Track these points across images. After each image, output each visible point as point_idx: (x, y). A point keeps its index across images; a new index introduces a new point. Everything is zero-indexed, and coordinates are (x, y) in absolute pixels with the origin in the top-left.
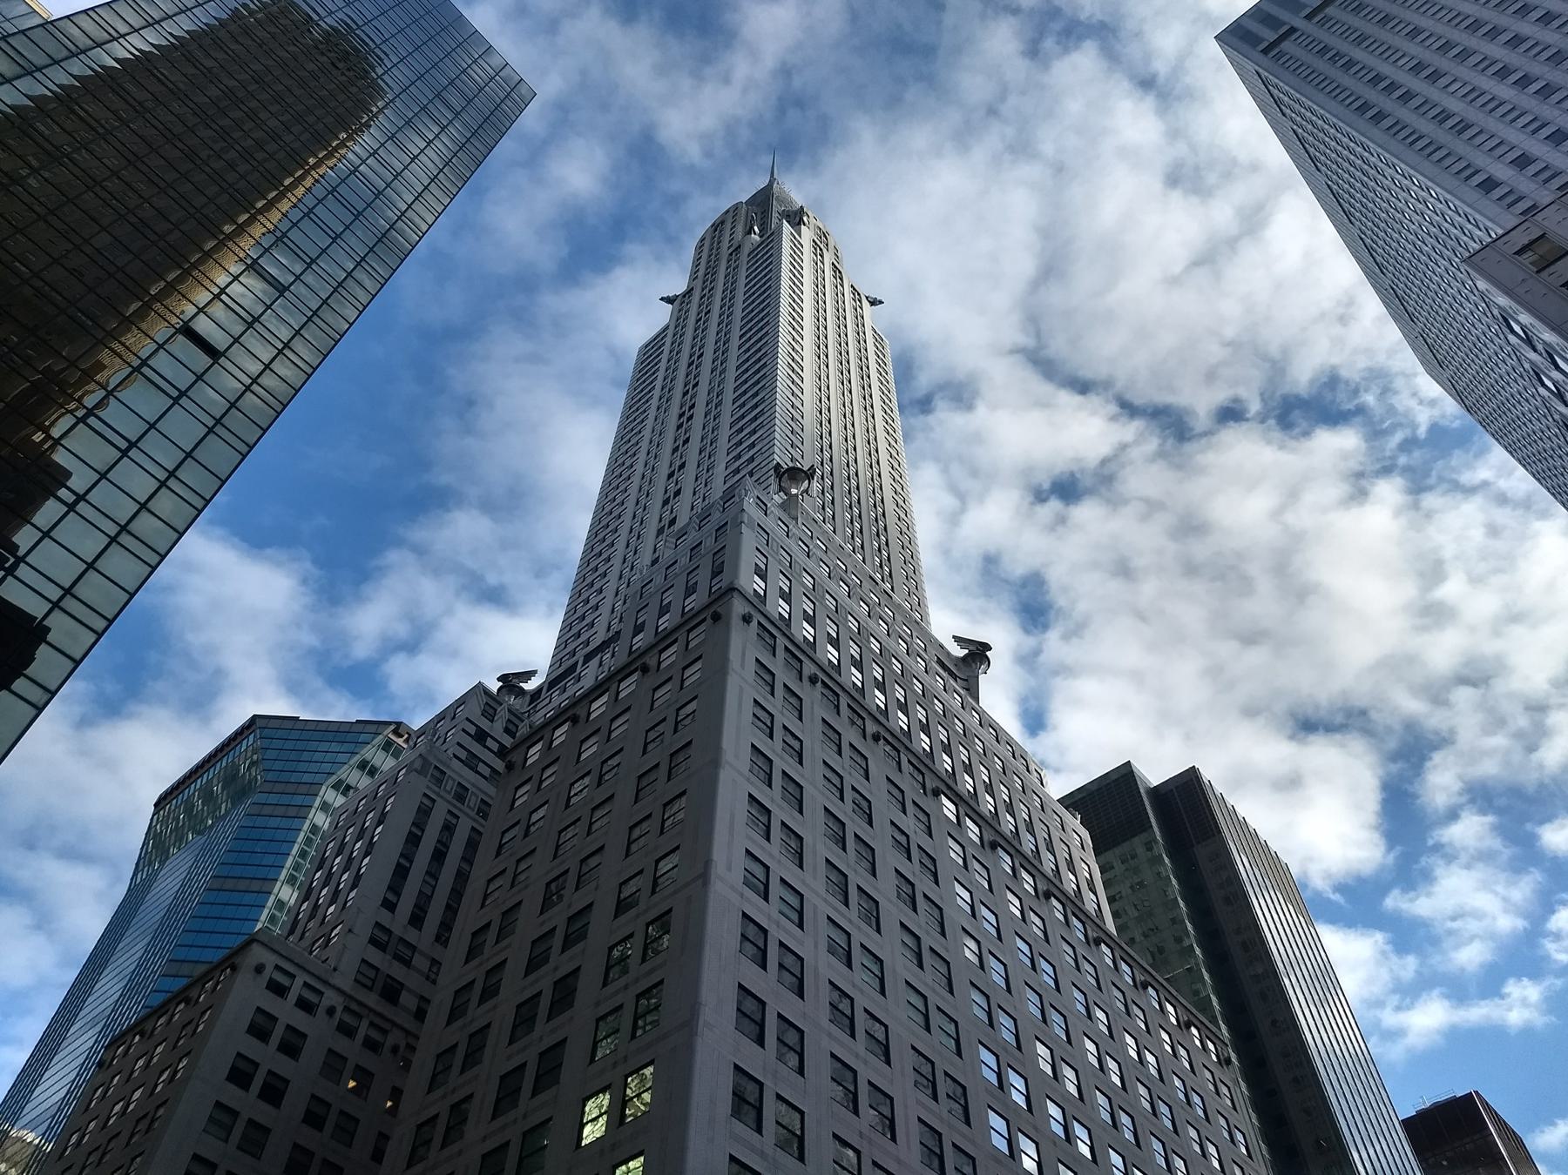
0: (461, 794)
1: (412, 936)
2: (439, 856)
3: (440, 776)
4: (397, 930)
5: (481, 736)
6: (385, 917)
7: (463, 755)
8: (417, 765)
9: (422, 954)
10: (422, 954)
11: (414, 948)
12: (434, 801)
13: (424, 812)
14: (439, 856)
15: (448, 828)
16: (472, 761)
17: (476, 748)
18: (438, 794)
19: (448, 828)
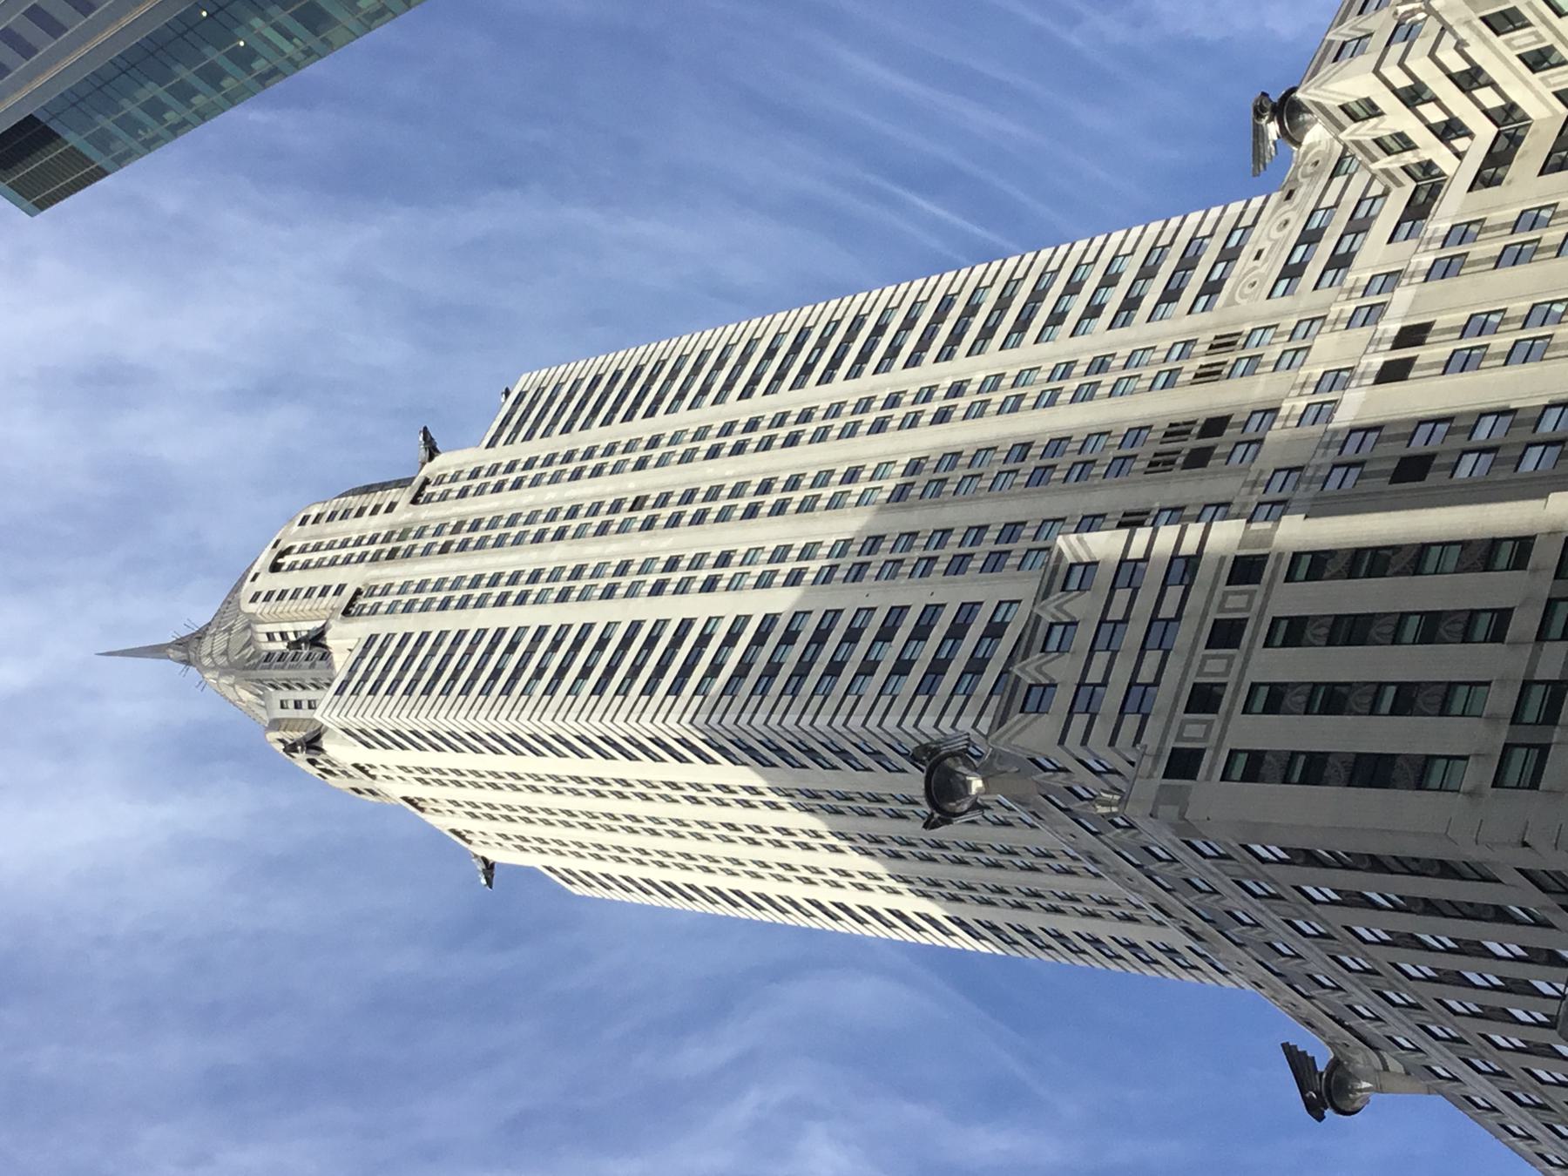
0: (1204, 699)
1: (1502, 700)
2: (1331, 699)
3: (1183, 764)
4: (1503, 735)
5: (1086, 696)
6: (1478, 774)
7: (1131, 722)
8: (1171, 811)
9: (1535, 657)
10: (1535, 657)
11: (1527, 685)
12: (1232, 752)
13: (1254, 766)
14: (1331, 699)
15: (1275, 699)
16: (1138, 696)
17: (1112, 699)
18: (1217, 750)
19: (1275, 699)
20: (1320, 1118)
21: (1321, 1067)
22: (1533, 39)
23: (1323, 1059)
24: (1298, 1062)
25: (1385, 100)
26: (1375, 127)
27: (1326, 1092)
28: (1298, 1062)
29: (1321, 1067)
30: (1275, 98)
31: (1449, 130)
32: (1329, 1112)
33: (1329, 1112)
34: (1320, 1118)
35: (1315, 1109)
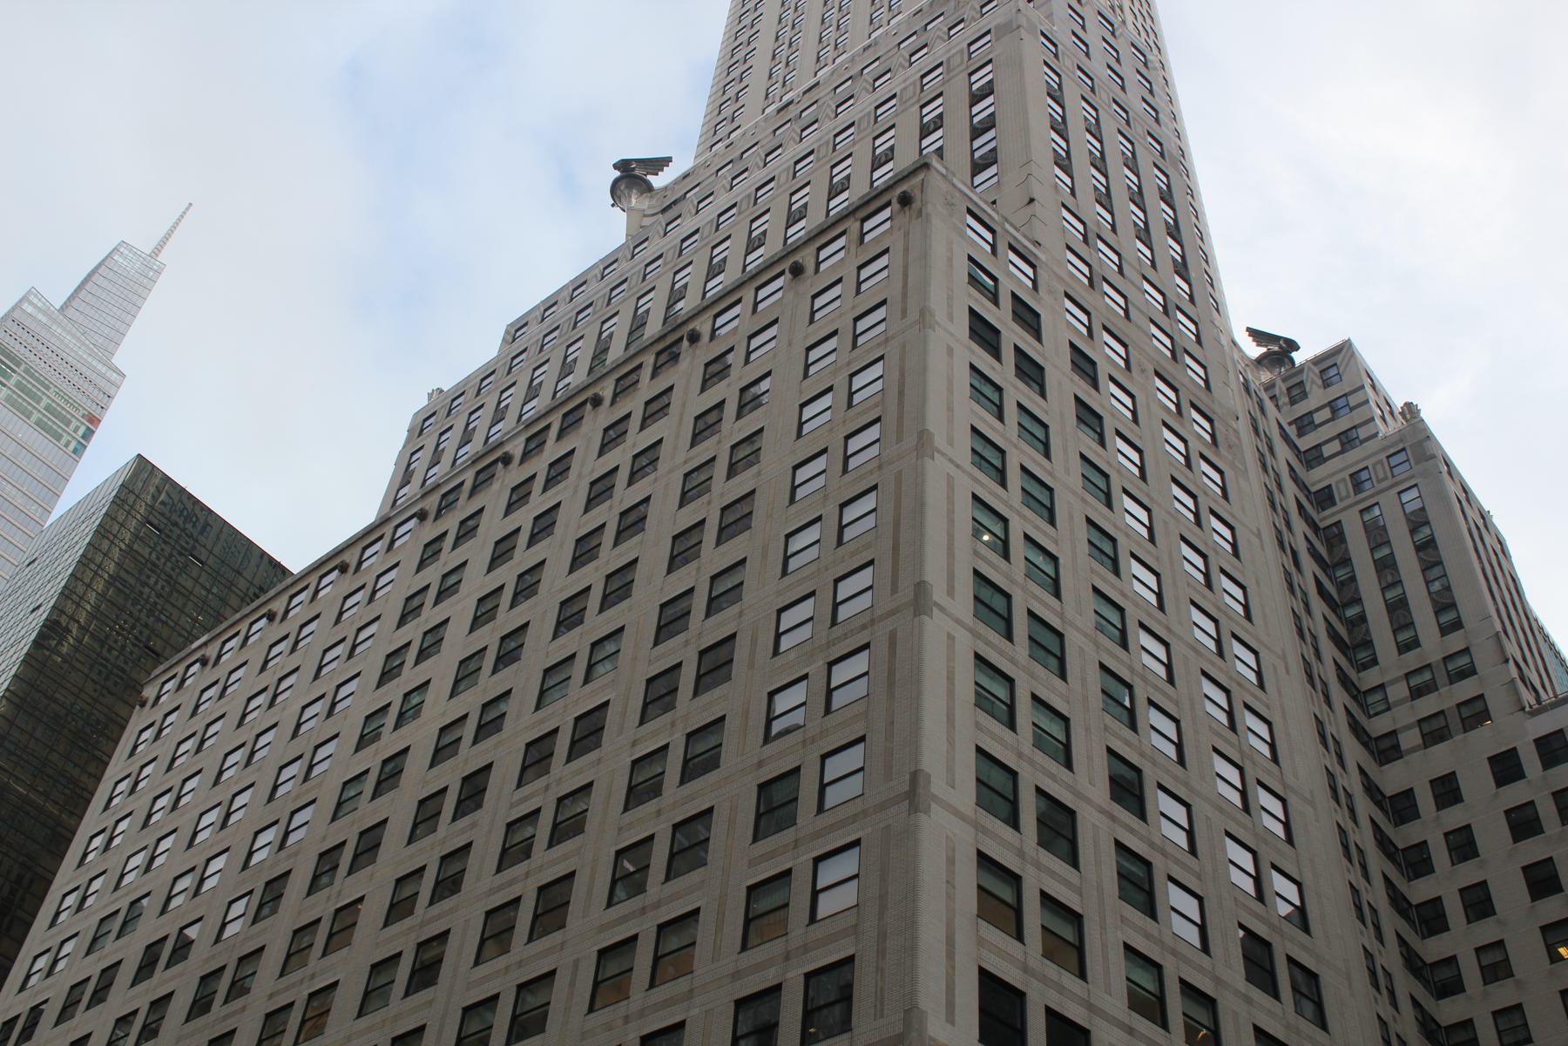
20: (616, 166)
21: (649, 178)
22: (1381, 475)
23: (658, 181)
24: (659, 164)
25: (1334, 392)
26: (1313, 382)
27: (631, 177)
28: (659, 164)
29: (649, 178)
30: (1294, 354)
31: (1304, 424)
32: (617, 174)
33: (617, 174)
34: (616, 166)
35: (624, 166)
